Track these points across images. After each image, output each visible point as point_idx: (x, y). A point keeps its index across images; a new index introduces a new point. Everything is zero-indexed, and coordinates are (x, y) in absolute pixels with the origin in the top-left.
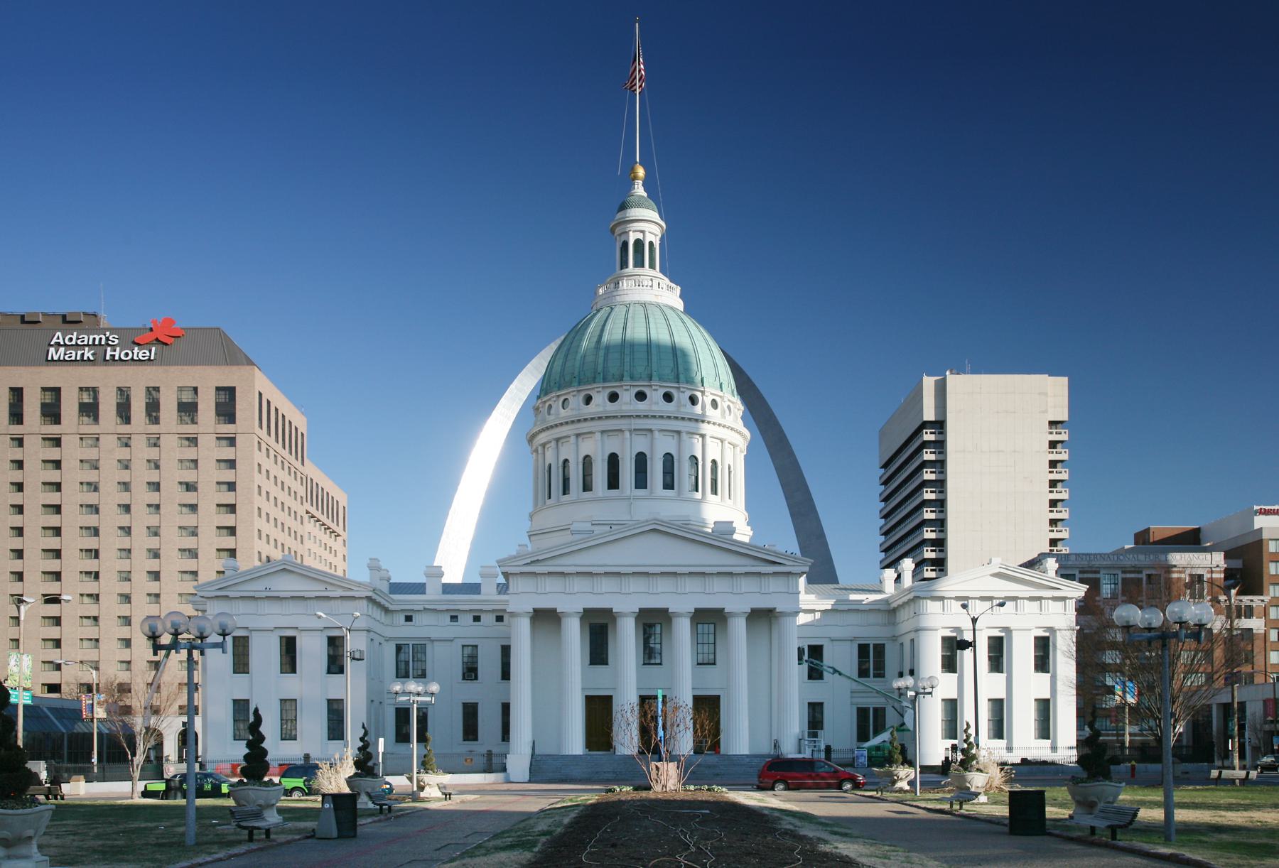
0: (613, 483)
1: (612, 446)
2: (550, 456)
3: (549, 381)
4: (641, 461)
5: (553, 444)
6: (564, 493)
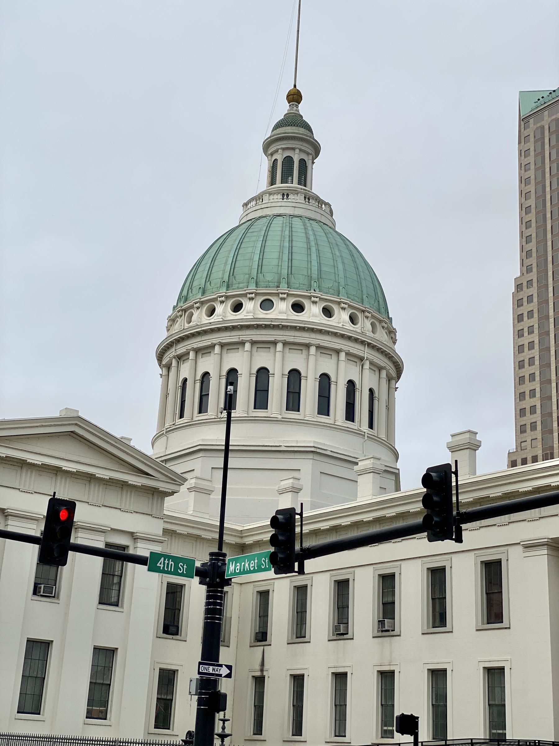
0: (261, 399)
1: (263, 359)
2: (186, 370)
3: (191, 288)
4: (294, 376)
5: (192, 355)
6: (200, 412)
